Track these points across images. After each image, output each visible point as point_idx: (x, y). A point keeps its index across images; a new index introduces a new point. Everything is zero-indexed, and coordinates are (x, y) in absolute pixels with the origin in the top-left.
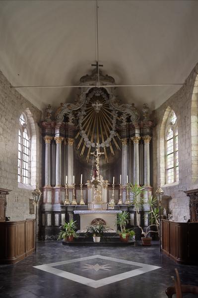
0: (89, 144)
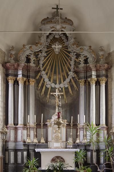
0: (50, 84)
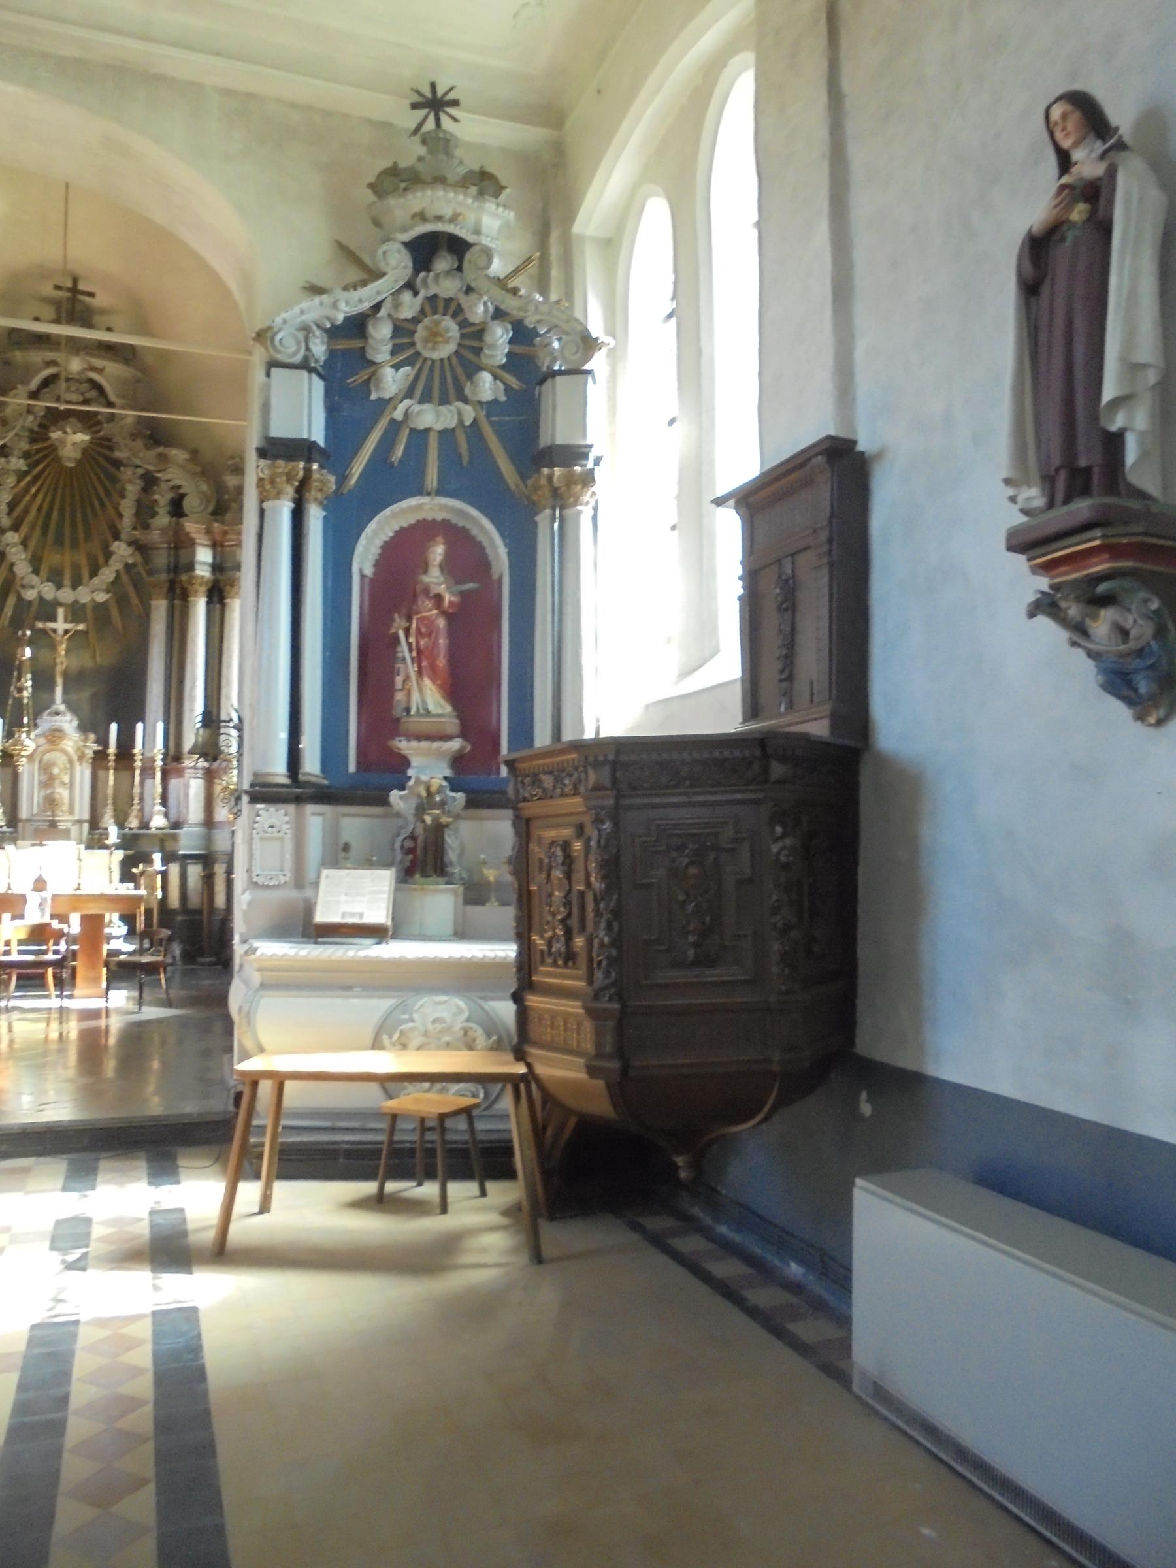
0: (37, 589)
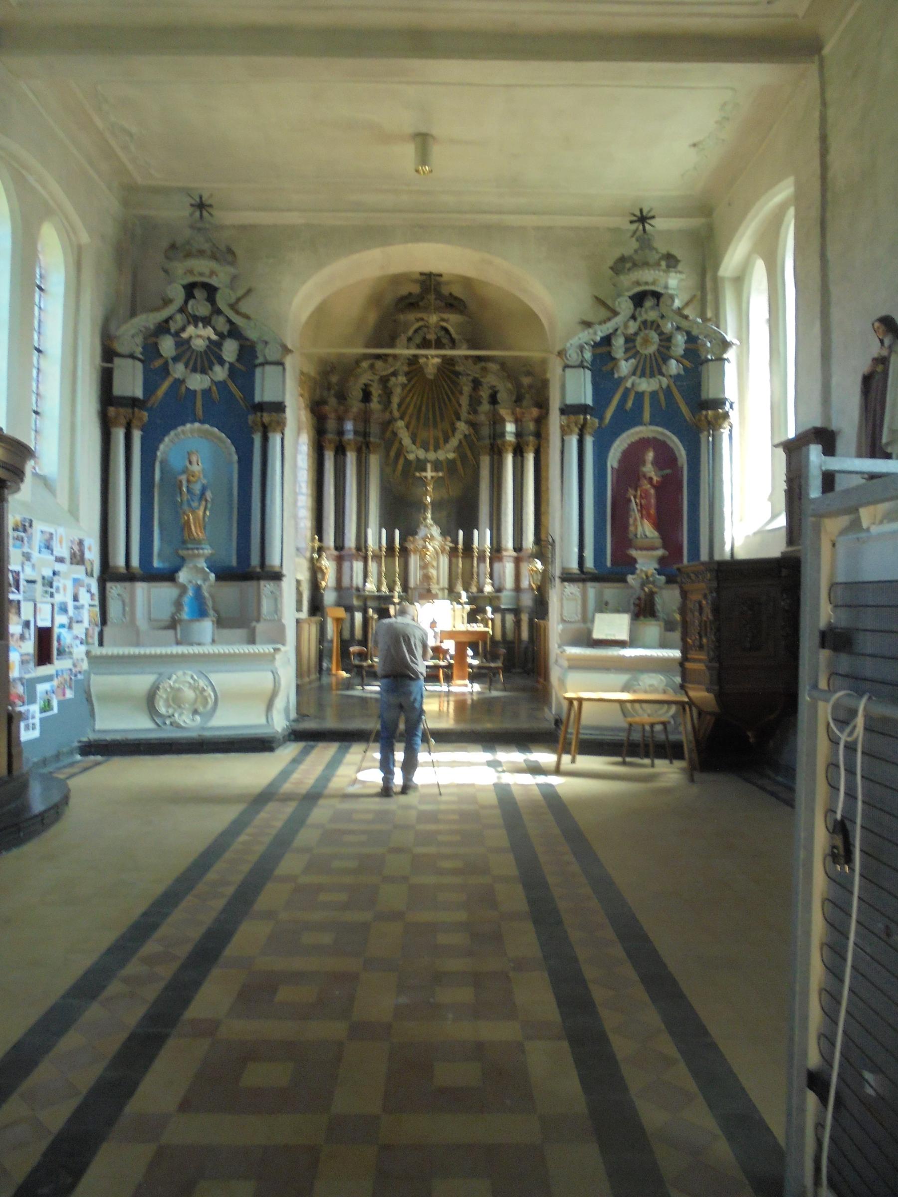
0: (415, 453)
